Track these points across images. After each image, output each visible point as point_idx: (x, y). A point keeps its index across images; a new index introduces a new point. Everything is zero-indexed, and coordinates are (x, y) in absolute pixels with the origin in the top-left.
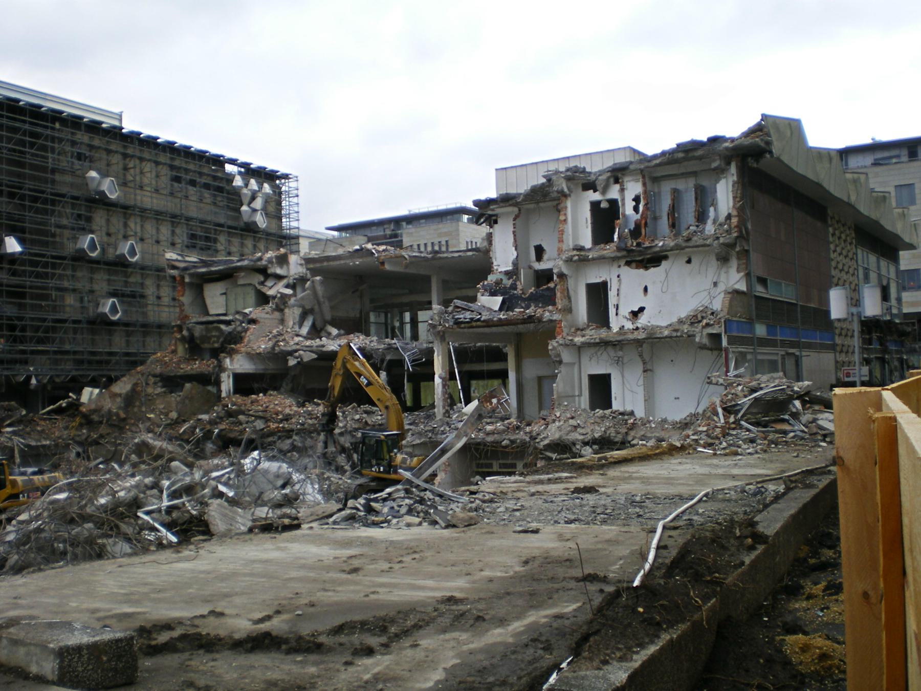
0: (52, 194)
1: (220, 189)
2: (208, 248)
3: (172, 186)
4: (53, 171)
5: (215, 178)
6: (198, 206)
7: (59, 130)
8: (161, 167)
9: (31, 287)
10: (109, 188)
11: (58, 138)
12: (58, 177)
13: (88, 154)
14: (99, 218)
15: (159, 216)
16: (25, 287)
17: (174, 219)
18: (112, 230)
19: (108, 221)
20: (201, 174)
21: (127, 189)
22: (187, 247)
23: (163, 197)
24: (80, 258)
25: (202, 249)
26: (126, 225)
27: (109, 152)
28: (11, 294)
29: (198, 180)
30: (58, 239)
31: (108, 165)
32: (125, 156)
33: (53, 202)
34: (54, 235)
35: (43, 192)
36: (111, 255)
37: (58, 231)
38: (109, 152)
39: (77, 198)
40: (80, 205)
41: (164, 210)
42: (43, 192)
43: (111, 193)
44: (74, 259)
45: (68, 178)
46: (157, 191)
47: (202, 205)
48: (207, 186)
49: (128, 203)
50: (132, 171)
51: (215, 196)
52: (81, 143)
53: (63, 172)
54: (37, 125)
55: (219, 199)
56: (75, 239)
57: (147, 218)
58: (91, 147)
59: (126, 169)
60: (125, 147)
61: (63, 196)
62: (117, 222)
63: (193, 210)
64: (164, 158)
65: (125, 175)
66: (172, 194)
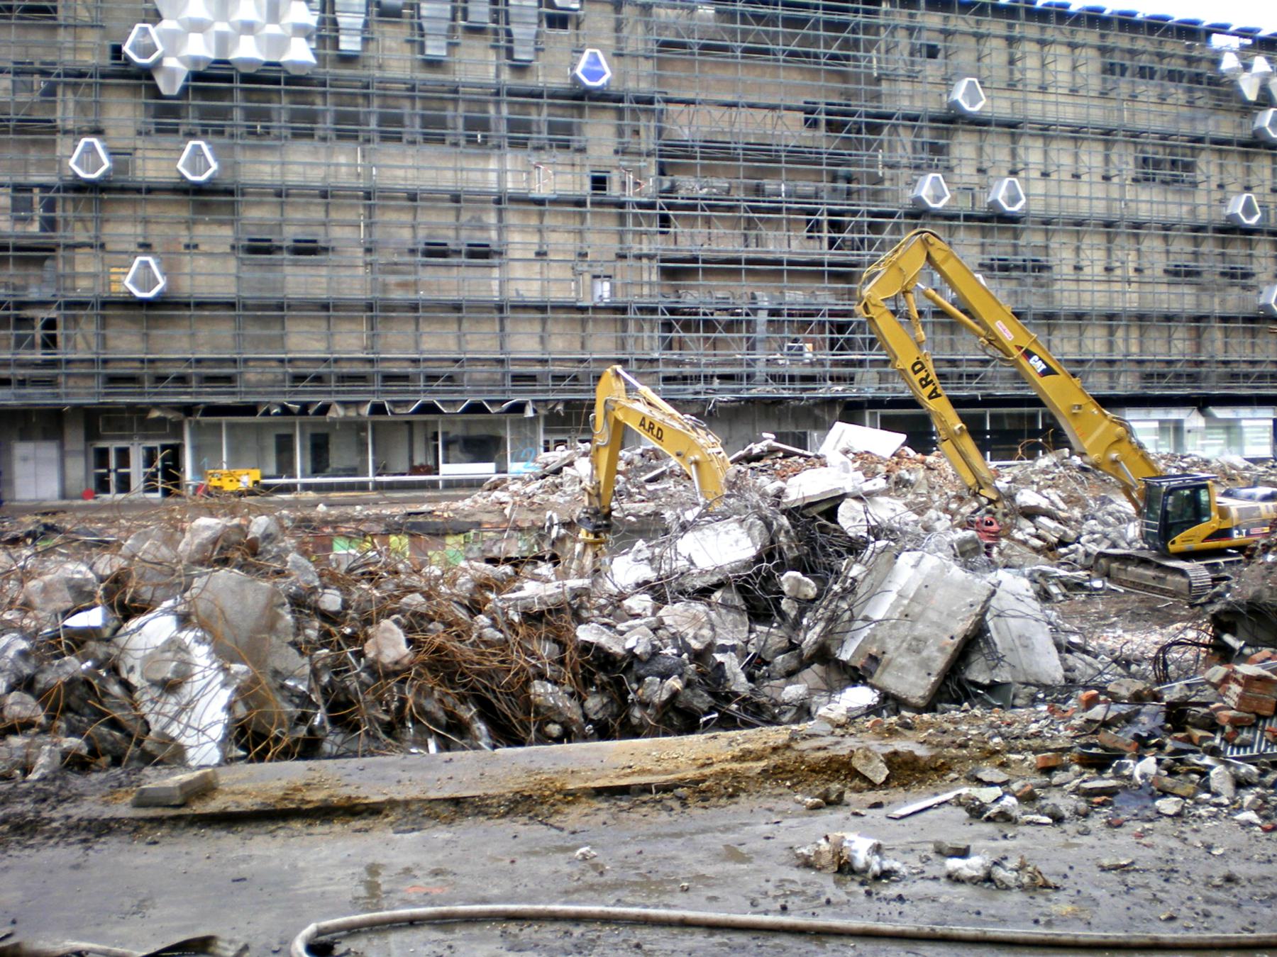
0: (868, 115)
1: (1197, 79)
2: (1175, 180)
3: (1104, 81)
4: (878, 80)
5: (1190, 60)
6: (1155, 110)
7: (886, 13)
8: (1077, 51)
9: (830, 264)
10: (966, 95)
11: (886, 26)
12: (884, 86)
13: (940, 45)
14: (963, 148)
15: (1076, 133)
16: (822, 264)
17: (1107, 135)
18: (985, 166)
19: (980, 150)
20: (1161, 56)
21: (1016, 95)
22: (1135, 180)
23: (1085, 101)
24: (918, 213)
25: (1164, 182)
26: (1014, 154)
27: (979, 37)
28: (835, 276)
29: (1157, 67)
30: (887, 184)
31: (979, 59)
32: (1011, 41)
33: (874, 129)
34: (880, 181)
35: (852, 114)
36: (981, 208)
37: (888, 173)
38: (979, 37)
39: (915, 118)
40: (921, 128)
41: (1084, 122)
42: (852, 114)
43: (972, 104)
44: (909, 215)
45: (905, 87)
46: (1074, 91)
47: (1165, 108)
48: (1173, 76)
49: (1018, 117)
50: (1019, 64)
51: (1190, 90)
52: (920, 29)
53: (892, 78)
54: (846, 10)
55: (1198, 94)
56: (912, 184)
57: (1052, 137)
58: (947, 33)
59: (1012, 62)
60: (1011, 26)
61: (889, 116)
62: (998, 150)
63: (1129, 116)
64: (1090, 36)
65: (1011, 72)
66: (1103, 95)
